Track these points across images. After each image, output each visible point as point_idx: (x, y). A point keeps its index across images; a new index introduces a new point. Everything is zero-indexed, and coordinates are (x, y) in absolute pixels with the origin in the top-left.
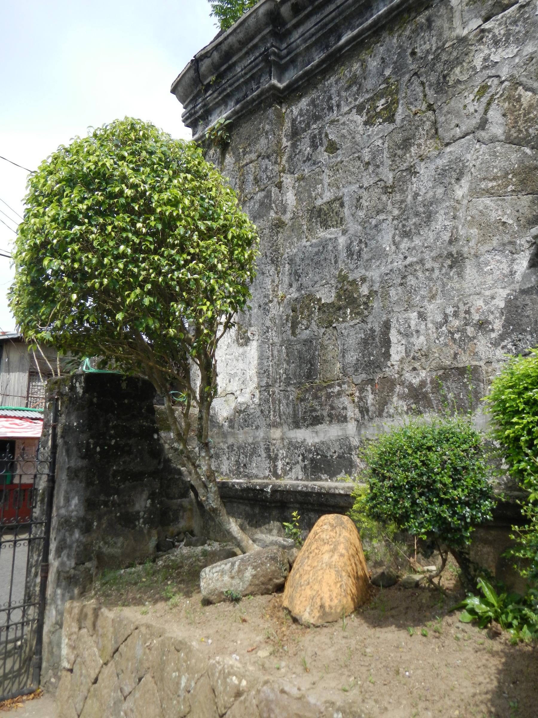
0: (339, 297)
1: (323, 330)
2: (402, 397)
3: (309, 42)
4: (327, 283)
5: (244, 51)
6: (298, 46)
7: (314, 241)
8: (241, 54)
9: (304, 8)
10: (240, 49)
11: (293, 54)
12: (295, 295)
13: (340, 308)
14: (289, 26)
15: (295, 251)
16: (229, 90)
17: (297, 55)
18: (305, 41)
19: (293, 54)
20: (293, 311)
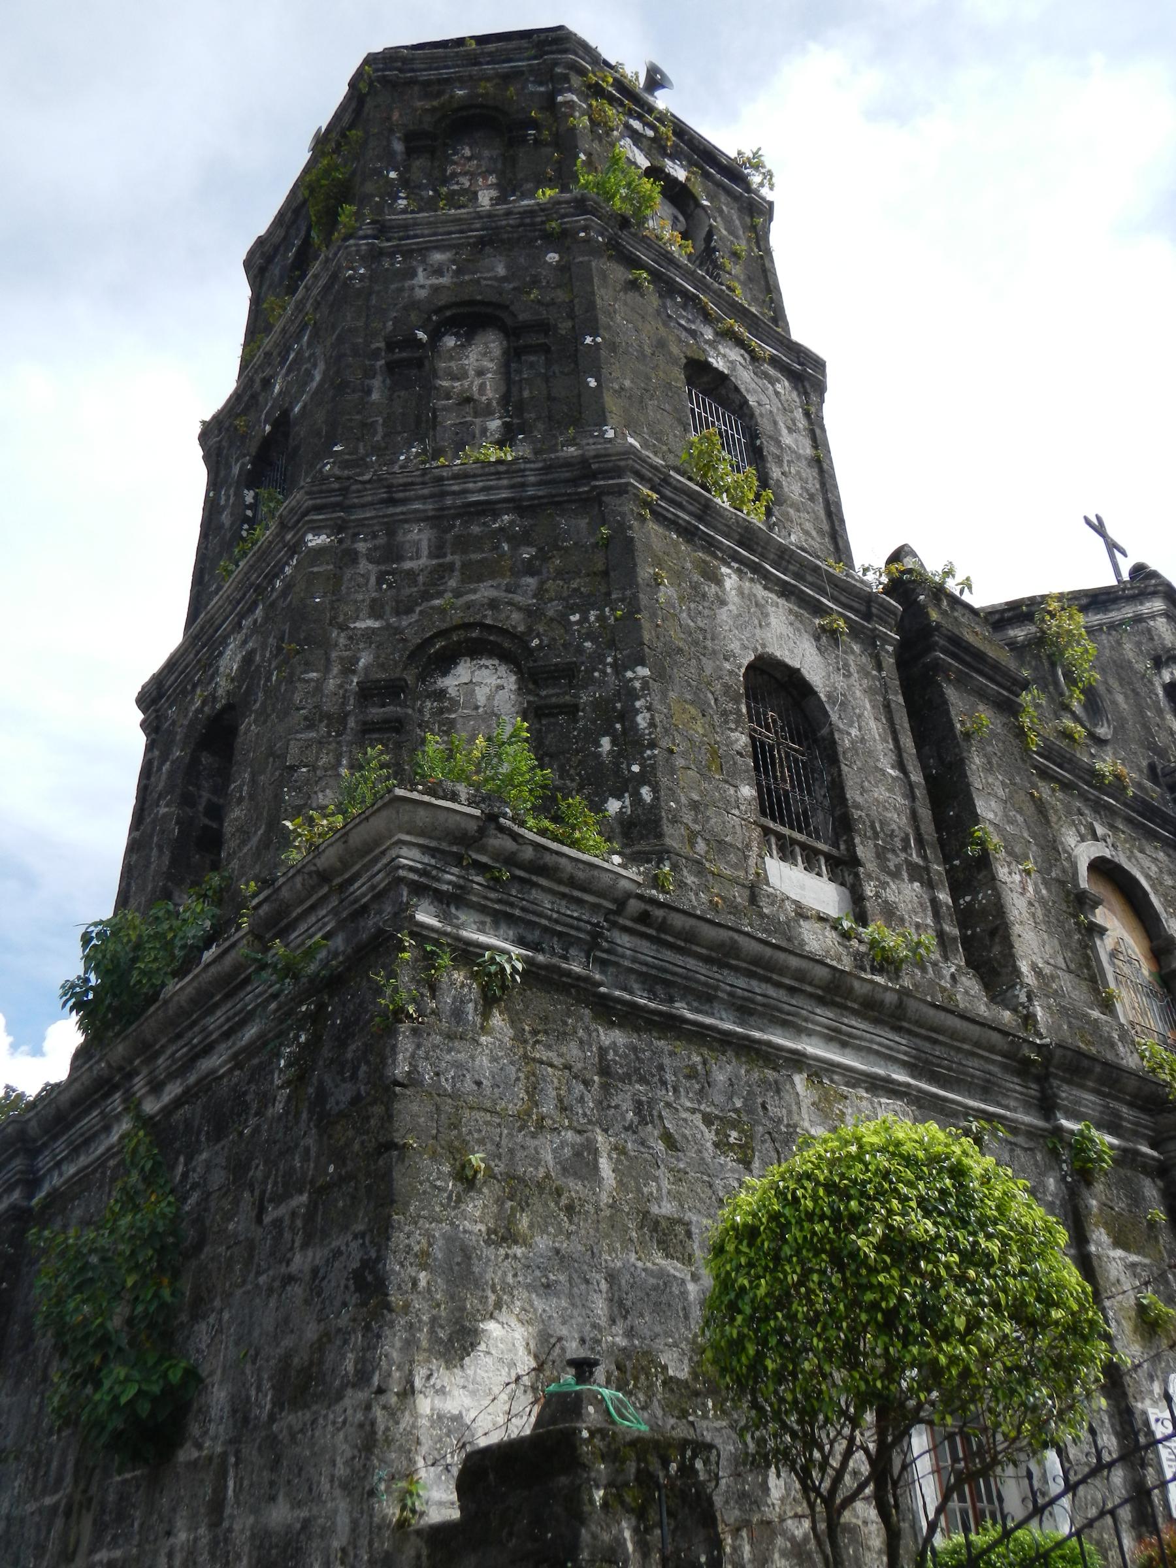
0: (695, 1375)
1: (672, 1421)
2: (784, 1554)
3: (636, 966)
4: (675, 1345)
5: (562, 889)
6: (623, 956)
7: (649, 1265)
8: (556, 887)
9: (649, 926)
10: (560, 882)
11: (613, 958)
12: (622, 1342)
13: (697, 1394)
14: (621, 921)
15: (619, 1264)
16: (517, 912)
17: (616, 964)
18: (634, 960)
19: (613, 958)
20: (618, 1368)
